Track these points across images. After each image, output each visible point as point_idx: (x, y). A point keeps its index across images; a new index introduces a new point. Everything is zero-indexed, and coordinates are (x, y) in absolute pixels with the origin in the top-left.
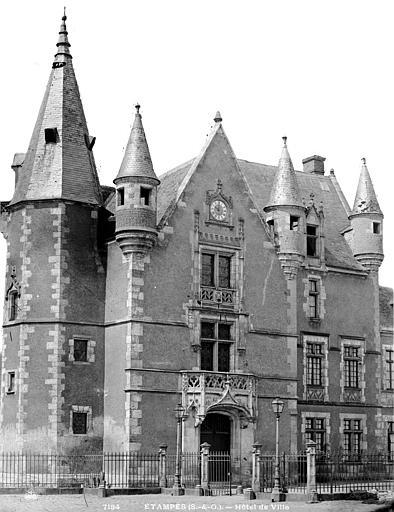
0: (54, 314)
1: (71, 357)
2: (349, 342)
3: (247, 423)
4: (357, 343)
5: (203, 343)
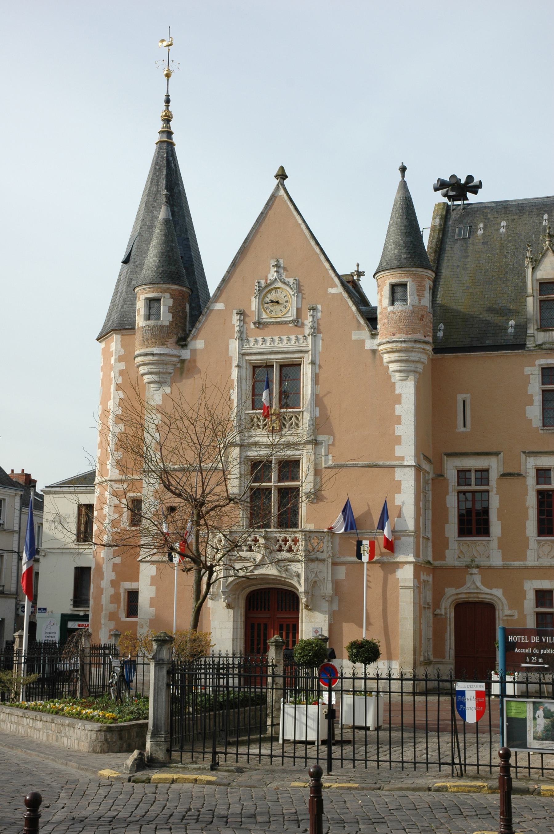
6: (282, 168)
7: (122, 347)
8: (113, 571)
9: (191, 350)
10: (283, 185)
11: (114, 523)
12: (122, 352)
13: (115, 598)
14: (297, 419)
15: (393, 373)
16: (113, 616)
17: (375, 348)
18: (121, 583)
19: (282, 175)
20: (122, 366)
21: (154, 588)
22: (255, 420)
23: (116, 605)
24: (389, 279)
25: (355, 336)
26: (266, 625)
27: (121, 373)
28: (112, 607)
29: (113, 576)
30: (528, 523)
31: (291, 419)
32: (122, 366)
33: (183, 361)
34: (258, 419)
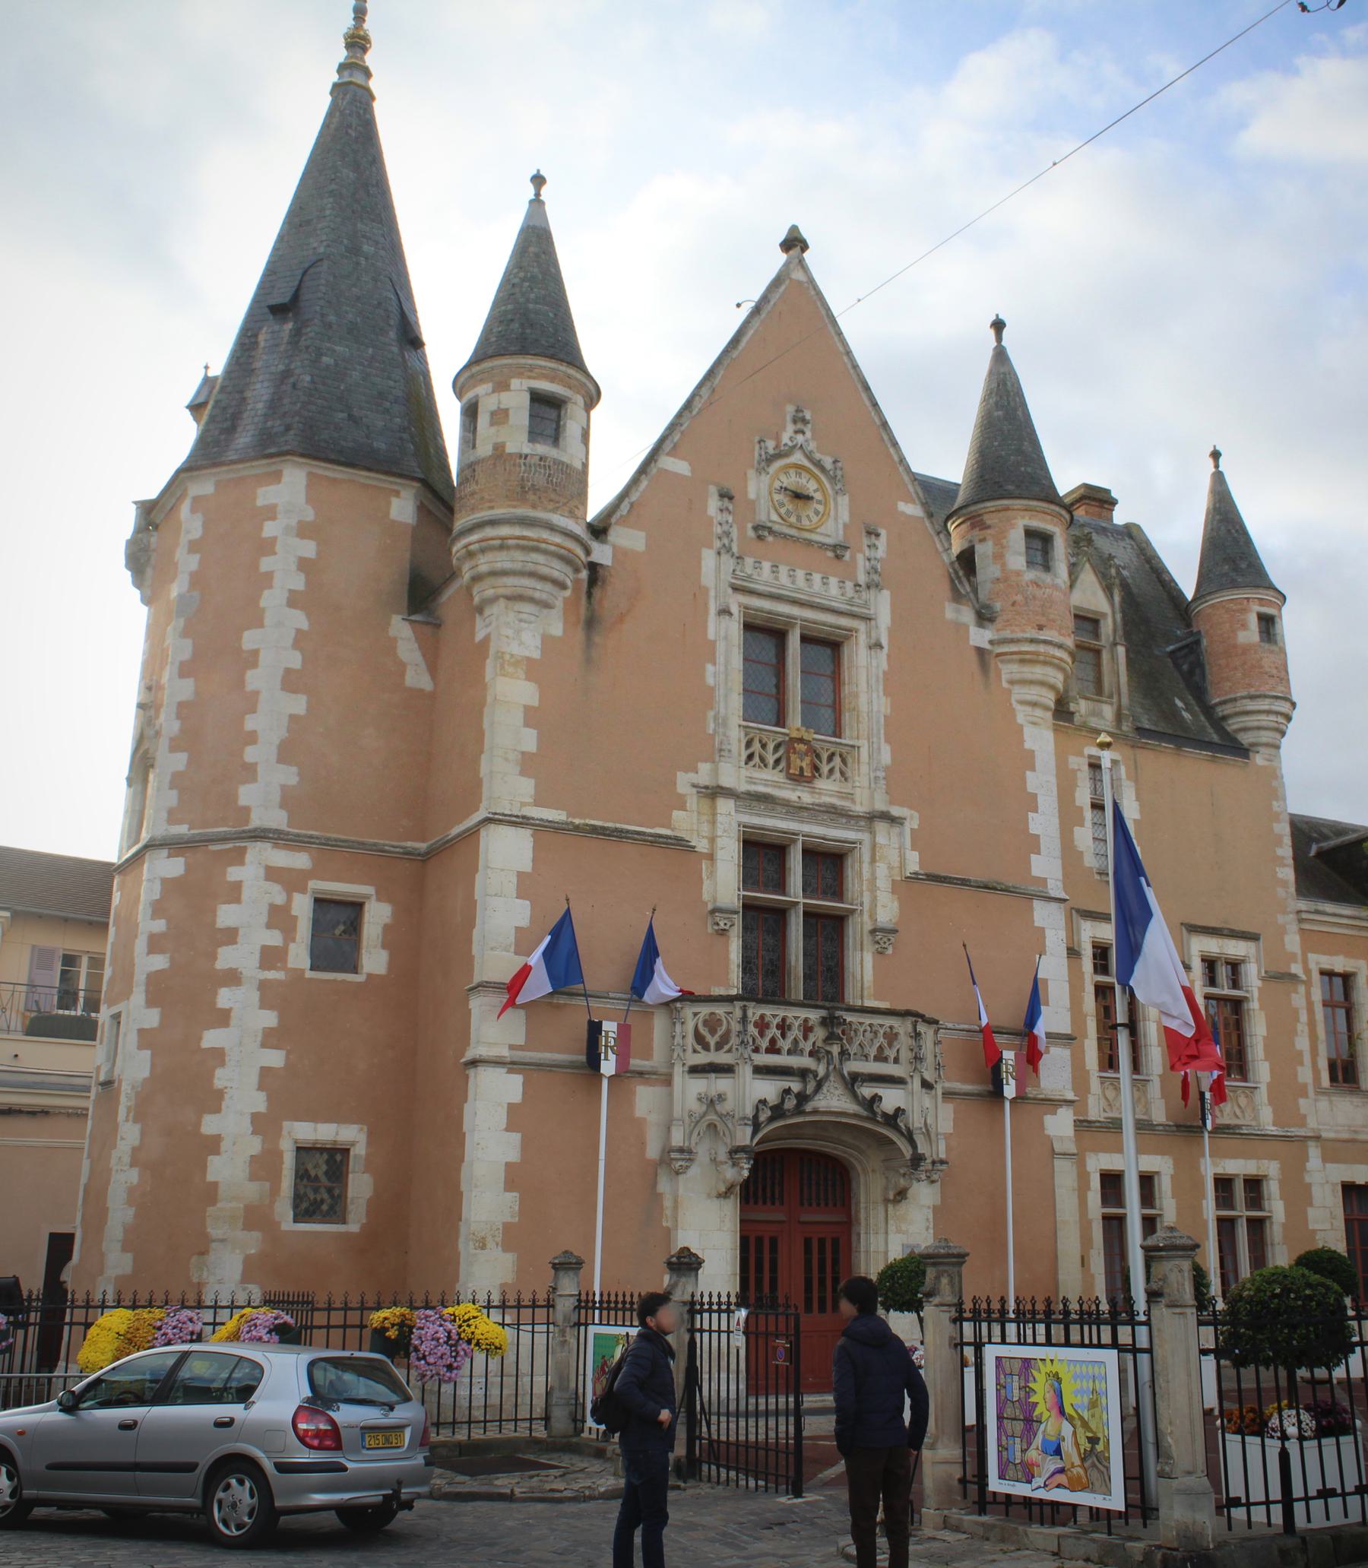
0: (247, 810)
1: (299, 956)
2: (1213, 946)
3: (902, 1182)
4: (1235, 948)
5: (749, 907)
6: (794, 229)
7: (309, 501)
8: (260, 1088)
9: (614, 547)
10: (801, 263)
11: (271, 957)
12: (309, 515)
13: (263, 1166)
14: (844, 761)
15: (1018, 707)
16: (256, 1218)
17: (988, 646)
18: (286, 1124)
19: (794, 243)
20: (308, 549)
21: (516, 1137)
22: (756, 746)
23: (267, 1185)
24: (1023, 517)
25: (950, 611)
26: (774, 1242)
27: (304, 565)
28: (253, 1191)
29: (259, 1102)
30: (1087, 1042)
31: (830, 758)
32: (308, 549)
33: (593, 567)
34: (764, 746)
